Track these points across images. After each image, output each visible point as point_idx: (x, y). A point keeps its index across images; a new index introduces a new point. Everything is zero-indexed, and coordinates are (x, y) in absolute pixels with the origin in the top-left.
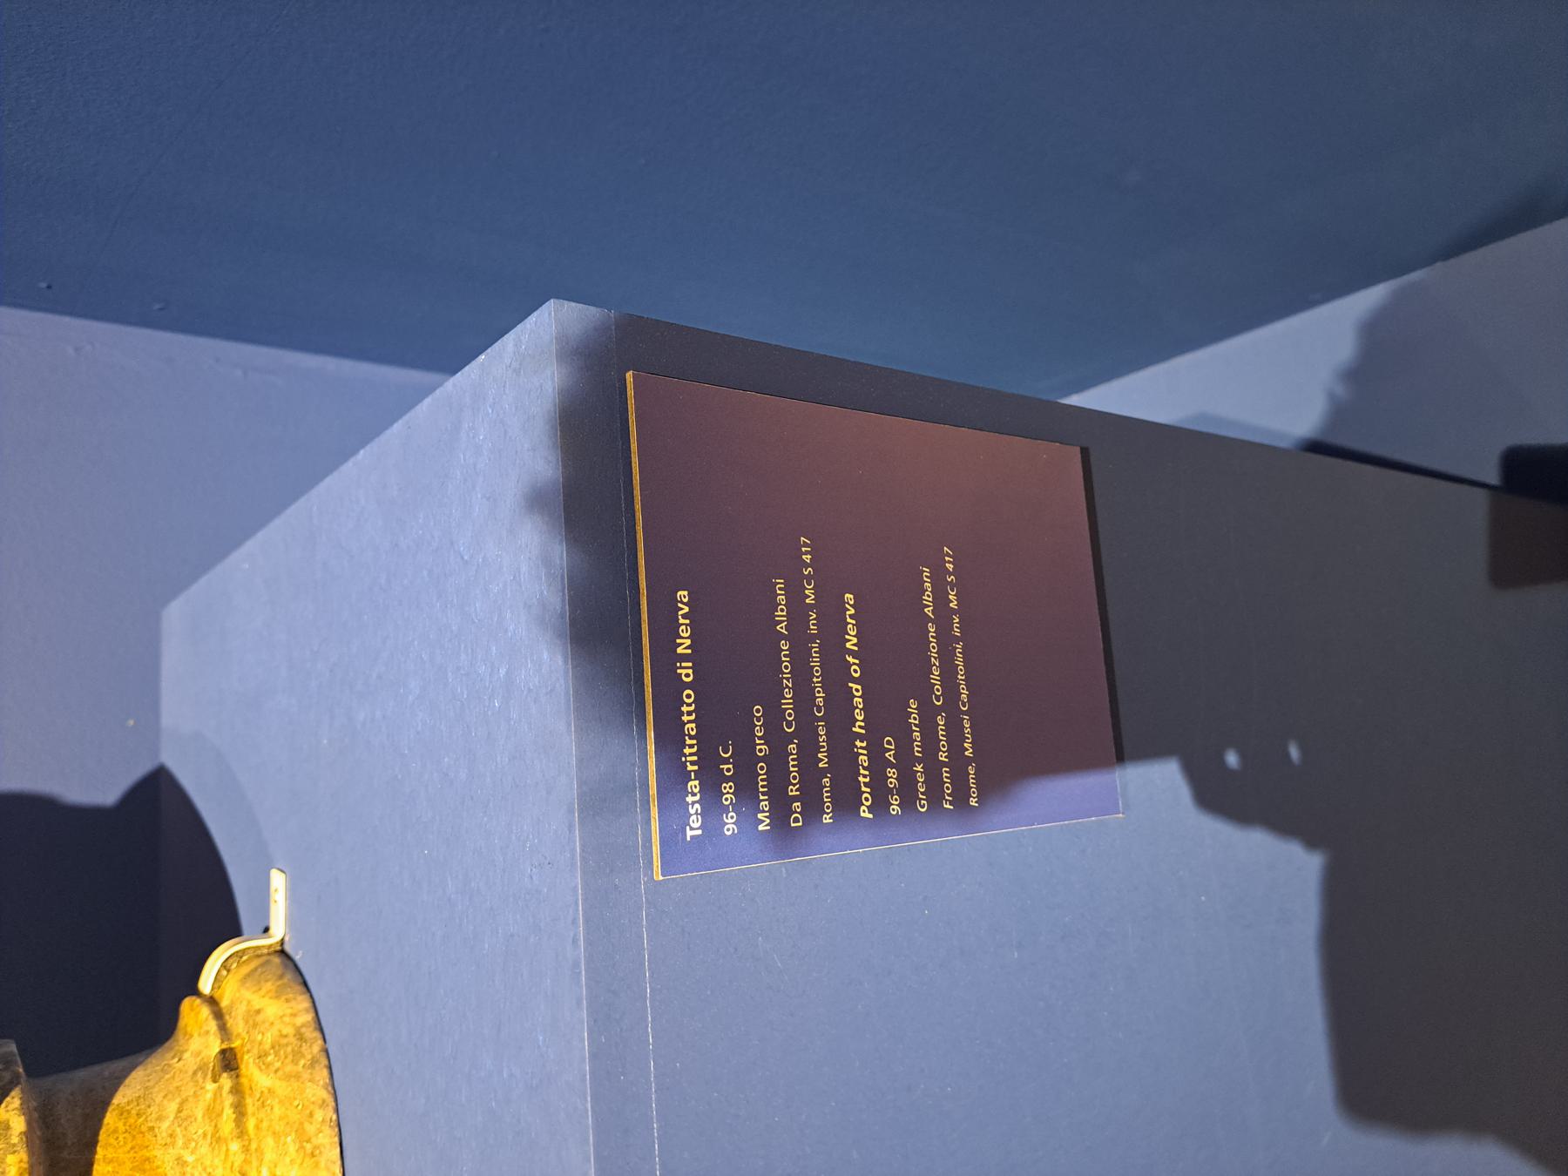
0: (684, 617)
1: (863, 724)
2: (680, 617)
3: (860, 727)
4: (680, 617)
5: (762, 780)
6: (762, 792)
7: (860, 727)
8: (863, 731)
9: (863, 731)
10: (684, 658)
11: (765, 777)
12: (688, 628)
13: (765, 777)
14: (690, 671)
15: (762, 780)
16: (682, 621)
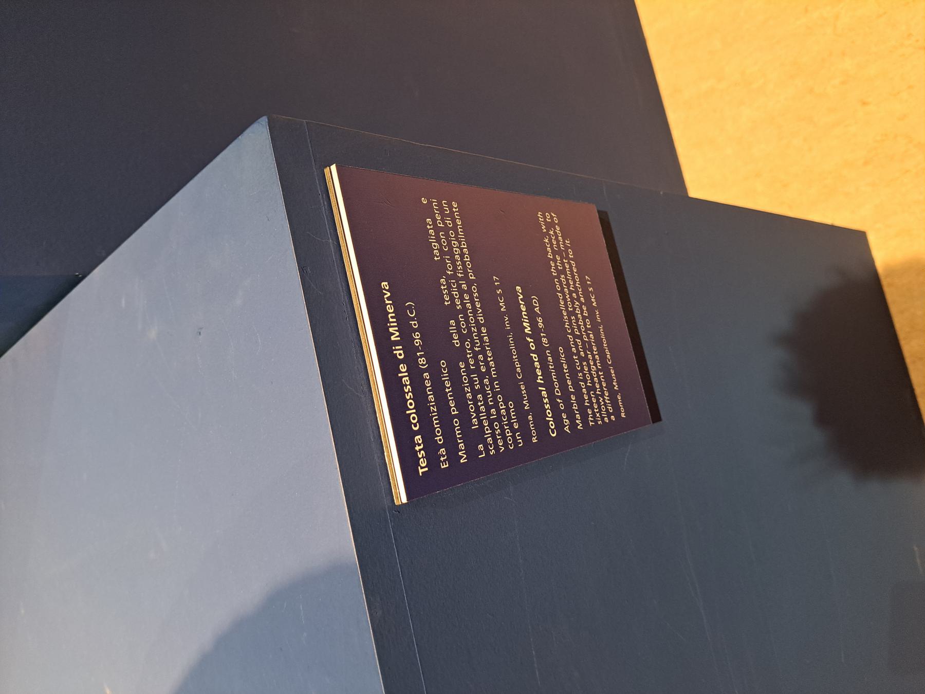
0: (388, 299)
1: (541, 377)
2: (386, 299)
3: (541, 379)
4: (386, 299)
5: (458, 430)
6: (458, 438)
7: (541, 379)
8: (542, 382)
9: (542, 382)
10: (396, 343)
11: (459, 427)
12: (392, 306)
13: (459, 427)
14: (401, 352)
15: (458, 430)
16: (387, 302)
